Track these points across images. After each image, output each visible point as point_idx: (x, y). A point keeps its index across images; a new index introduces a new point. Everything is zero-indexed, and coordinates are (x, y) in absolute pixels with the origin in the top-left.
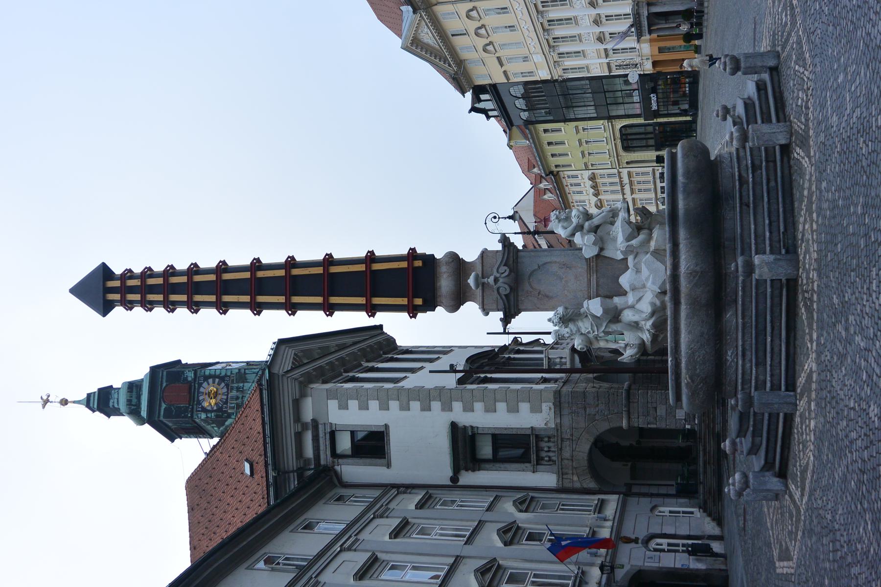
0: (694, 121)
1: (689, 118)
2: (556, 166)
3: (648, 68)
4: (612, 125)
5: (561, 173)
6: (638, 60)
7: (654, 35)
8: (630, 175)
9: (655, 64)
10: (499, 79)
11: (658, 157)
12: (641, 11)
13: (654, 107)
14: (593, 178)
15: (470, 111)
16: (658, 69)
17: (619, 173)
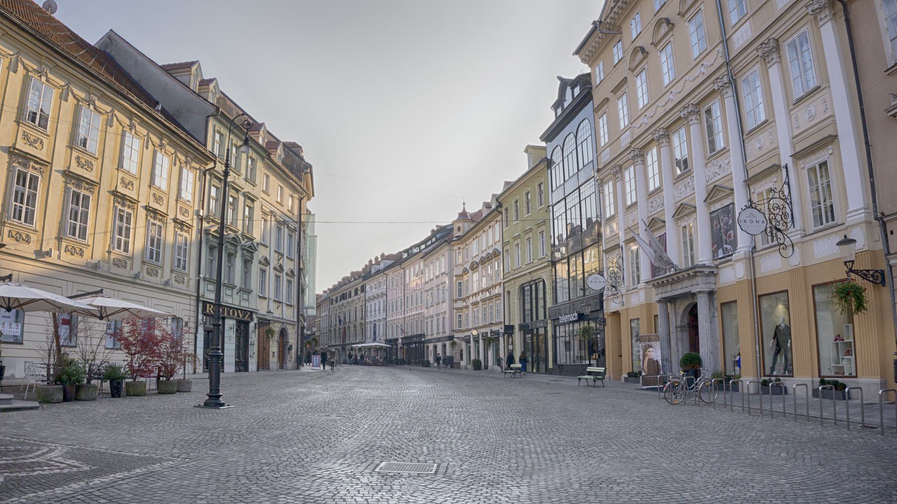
0: (548, 371)
1: (551, 366)
2: (506, 209)
3: (611, 306)
4: (545, 267)
5: (499, 218)
6: (623, 289)
7: (658, 309)
8: (498, 295)
9: (616, 314)
10: (598, 96)
11: (512, 327)
12: (699, 279)
13: (563, 319)
14: (496, 254)
15: (559, 78)
16: (609, 321)
17: (500, 284)
